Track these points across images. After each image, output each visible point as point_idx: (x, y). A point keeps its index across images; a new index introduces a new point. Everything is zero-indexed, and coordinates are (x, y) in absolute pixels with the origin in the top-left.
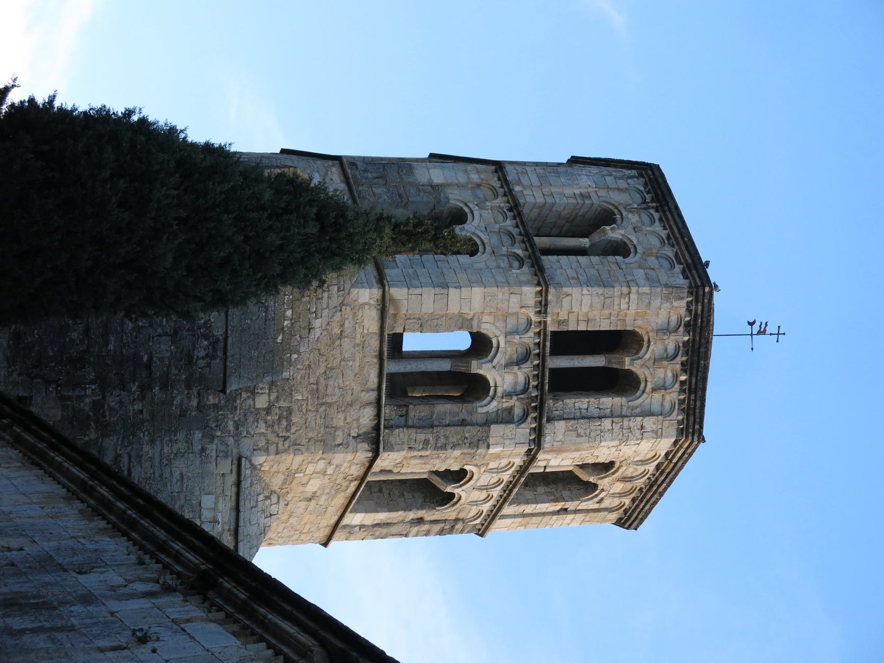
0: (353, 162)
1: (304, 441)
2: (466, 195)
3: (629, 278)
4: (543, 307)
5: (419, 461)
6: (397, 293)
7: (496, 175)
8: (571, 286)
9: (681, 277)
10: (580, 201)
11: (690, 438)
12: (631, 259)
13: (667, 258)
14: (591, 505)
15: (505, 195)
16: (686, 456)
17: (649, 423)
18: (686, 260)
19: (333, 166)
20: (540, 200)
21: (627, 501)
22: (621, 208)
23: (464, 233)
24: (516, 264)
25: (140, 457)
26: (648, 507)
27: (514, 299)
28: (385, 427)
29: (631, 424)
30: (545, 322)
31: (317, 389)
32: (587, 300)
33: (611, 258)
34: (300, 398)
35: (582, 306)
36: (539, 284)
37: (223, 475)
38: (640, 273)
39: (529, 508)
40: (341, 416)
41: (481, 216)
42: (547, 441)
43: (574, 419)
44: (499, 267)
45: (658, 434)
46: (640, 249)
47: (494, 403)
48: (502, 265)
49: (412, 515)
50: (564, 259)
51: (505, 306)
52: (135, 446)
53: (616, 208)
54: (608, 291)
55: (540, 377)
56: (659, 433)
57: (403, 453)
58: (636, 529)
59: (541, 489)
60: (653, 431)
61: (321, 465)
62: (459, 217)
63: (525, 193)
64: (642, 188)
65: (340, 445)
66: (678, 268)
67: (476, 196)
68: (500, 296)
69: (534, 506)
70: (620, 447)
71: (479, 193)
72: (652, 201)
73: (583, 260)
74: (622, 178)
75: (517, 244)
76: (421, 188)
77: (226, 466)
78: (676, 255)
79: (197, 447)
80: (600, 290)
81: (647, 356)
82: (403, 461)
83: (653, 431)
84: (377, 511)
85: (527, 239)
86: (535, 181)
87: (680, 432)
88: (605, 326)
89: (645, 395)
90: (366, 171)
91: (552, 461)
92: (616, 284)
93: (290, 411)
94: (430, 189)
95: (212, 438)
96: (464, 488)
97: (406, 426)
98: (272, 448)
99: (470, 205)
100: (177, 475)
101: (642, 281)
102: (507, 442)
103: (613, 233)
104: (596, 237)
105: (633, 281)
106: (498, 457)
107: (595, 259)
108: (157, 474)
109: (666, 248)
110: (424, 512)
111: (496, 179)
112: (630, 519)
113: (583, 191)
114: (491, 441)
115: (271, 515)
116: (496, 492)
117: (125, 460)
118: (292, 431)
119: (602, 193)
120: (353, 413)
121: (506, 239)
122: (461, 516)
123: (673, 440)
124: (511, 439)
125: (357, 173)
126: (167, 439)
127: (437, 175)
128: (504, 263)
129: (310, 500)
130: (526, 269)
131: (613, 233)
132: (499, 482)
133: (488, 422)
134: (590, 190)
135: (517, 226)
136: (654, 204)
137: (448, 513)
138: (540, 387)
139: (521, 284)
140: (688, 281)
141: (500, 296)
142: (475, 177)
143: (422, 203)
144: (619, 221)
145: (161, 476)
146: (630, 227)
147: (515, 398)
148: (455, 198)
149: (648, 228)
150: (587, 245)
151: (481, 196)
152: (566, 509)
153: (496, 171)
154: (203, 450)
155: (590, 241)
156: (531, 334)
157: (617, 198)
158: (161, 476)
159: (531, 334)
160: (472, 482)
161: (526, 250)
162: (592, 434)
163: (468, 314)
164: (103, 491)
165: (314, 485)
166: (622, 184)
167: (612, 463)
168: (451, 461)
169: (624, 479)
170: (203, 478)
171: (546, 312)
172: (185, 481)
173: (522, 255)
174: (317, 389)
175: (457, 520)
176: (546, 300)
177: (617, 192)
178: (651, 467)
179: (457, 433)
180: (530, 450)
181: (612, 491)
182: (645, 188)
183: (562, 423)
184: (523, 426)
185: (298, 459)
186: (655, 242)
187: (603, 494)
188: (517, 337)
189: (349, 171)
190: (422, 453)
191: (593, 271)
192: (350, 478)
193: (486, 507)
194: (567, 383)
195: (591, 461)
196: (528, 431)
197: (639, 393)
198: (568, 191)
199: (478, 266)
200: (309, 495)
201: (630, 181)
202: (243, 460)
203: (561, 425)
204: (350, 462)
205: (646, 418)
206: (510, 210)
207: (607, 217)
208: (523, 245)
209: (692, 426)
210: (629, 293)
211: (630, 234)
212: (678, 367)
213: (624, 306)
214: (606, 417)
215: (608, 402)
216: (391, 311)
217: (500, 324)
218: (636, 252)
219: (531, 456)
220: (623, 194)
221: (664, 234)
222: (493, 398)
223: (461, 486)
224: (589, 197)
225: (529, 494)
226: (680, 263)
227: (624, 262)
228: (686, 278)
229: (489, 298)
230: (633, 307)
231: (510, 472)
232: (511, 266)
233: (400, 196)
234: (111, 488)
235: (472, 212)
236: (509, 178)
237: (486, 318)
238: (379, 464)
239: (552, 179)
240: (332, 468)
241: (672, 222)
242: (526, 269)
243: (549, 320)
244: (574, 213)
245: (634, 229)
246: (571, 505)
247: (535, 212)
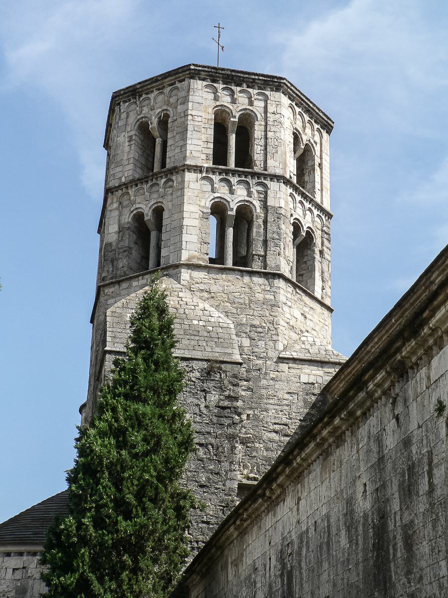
0: (101, 278)
1: (271, 318)
2: (126, 212)
3: (182, 115)
4: (197, 169)
5: (287, 249)
6: (185, 257)
7: (114, 193)
8: (186, 150)
9: (183, 82)
10: (134, 142)
11: (282, 85)
12: (171, 114)
13: (171, 91)
14: (317, 148)
15: (127, 188)
16: (292, 88)
17: (271, 109)
18: (173, 80)
19: (104, 291)
20: (131, 166)
21: (316, 126)
22: (139, 117)
23: (150, 214)
24: (170, 183)
25: (275, 418)
26: (321, 114)
27: (192, 185)
28: (266, 269)
29: (272, 120)
30: (207, 168)
31: (240, 308)
32: (195, 142)
33: (170, 125)
34: (245, 319)
35: (198, 146)
36: (184, 171)
37: (289, 368)
38: (180, 108)
39: (318, 186)
40: (257, 295)
41: (139, 203)
42: (279, 172)
43: (266, 155)
44: (172, 194)
45: (278, 104)
46: (165, 107)
47: (254, 202)
48: (171, 192)
49: (317, 256)
50: (168, 154)
51: (196, 192)
52: (269, 420)
53: (138, 121)
54: (190, 128)
55: (240, 174)
56: (278, 103)
57: (282, 259)
58: (333, 123)
59: (306, 178)
60: (277, 107)
61: (286, 309)
62: (139, 217)
63: (126, 175)
64: (127, 104)
65: (275, 297)
66: (178, 85)
67: (126, 207)
68: (189, 194)
69: (316, 183)
70: (285, 128)
71: (125, 204)
72: (135, 98)
73: (170, 142)
74: (120, 116)
75: (158, 182)
76: (120, 239)
77: (284, 367)
79: (271, 382)
80: (189, 133)
81: (231, 107)
82: (285, 259)
83: (277, 107)
84: (314, 279)
85: (156, 176)
86: (120, 169)
87: (278, 90)
88: (211, 132)
89: (254, 110)
90: (108, 271)
91: (291, 169)
92: (186, 123)
93: (253, 326)
94: (120, 233)
95: (266, 374)
96: (303, 225)
97: (265, 256)
98: (275, 338)
100: (287, 396)
101: (184, 107)
102: (278, 196)
103: (154, 124)
104: (156, 134)
105: (184, 112)
106: (287, 202)
107: (169, 135)
108: (286, 408)
109: (165, 91)
110: (316, 250)
111: (117, 193)
112: (327, 126)
113: (127, 140)
114: (277, 205)
115: (314, 341)
116: (307, 205)
117: (277, 427)
118: (265, 325)
119: (129, 129)
120: (257, 289)
121: (154, 189)
122: (320, 227)
123: (282, 95)
124: (277, 193)
125: (109, 276)
126: (265, 401)
127: (112, 228)
128: (170, 191)
129: (305, 317)
130: (174, 178)
131: (154, 124)
132: (301, 202)
133: (265, 207)
134: (126, 136)
135: (147, 182)
136: (137, 97)
137: (318, 235)
138: (246, 174)
139: (183, 181)
140: (186, 79)
141: (189, 194)
142: (115, 205)
143: (129, 240)
144: (147, 119)
145: (288, 405)
146: (151, 112)
147: (252, 190)
148: (127, 218)
149: (152, 101)
150: (161, 140)
151: (127, 202)
152: (319, 164)
153: (112, 193)
154: (273, 379)
155: (158, 137)
156: (213, 177)
157: (132, 119)
158: (288, 405)
159: (213, 177)
160: (301, 219)
161: (162, 177)
162: (276, 144)
163: (200, 215)
164: (325, 433)
165: (297, 314)
166: (124, 116)
167: (294, 133)
168: (287, 230)
169: (304, 128)
170: (290, 380)
171: (201, 167)
172: (291, 391)
173: (165, 179)
174: (240, 308)
175: (322, 231)
176: (194, 166)
177: (129, 119)
178: (298, 110)
179: (271, 226)
180: (284, 183)
181: (311, 136)
182: (127, 102)
183: (268, 161)
184: (269, 186)
185: (282, 323)
186: (161, 98)
187: (312, 141)
188: (215, 185)
189: (108, 282)
190: (282, 247)
191: (177, 137)
192: (294, 292)
193: (316, 212)
194: (244, 158)
195: (292, 146)
196: (272, 182)
197: (253, 114)
198: (127, 149)
199: (170, 207)
200: (303, 318)
201: (122, 111)
202: (281, 356)
203: (270, 162)
204: (284, 291)
205: (268, 110)
206: (137, 185)
207: (143, 128)
208: (159, 179)
209: (274, 83)
210: (192, 115)
211: (155, 113)
212: (239, 89)
213: (199, 119)
214: (266, 135)
215: (258, 132)
216: (195, 261)
217: (207, 195)
218: (167, 110)
219: (287, 182)
220: (131, 115)
221: (156, 92)
222: (251, 203)
223: (302, 226)
224: (131, 136)
225: (309, 186)
226: (174, 83)
227: (172, 117)
228: (184, 80)
229: (191, 202)
230: (200, 114)
231: (296, 196)
232: (171, 187)
233: (125, 251)
234: (323, 428)
235: (136, 209)
236: (117, 185)
237: (203, 204)
238: (287, 274)
239: (118, 158)
240: (288, 302)
241: (149, 87)
242: (174, 178)
243: (206, 165)
244: (141, 147)
245: (152, 110)
246: (317, 161)
247: (138, 170)
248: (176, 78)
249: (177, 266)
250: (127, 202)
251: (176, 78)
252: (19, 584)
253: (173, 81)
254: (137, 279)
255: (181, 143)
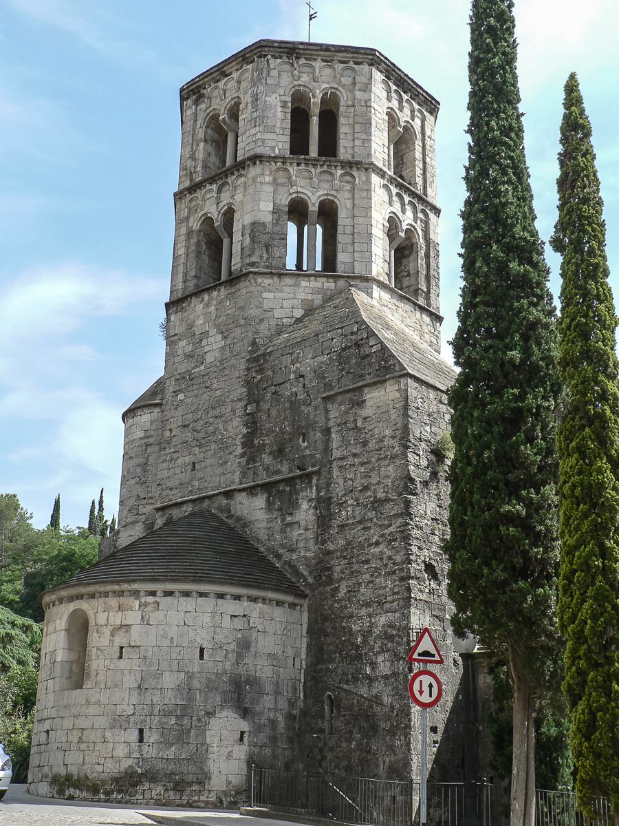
18: (349, 57)
67: (283, 185)
78: (343, 62)
99: (292, 191)
101: (366, 96)
130: (355, 174)
144: (307, 90)
151: (284, 180)
155: (316, 116)
166: (274, 73)
198: (280, 115)
218: (337, 89)
235: (297, 192)
241: (315, 53)
248: (353, 58)
249: (367, 279)
250: (284, 180)
251: (353, 58)
252: (240, 636)
253: (347, 59)
254: (307, 279)
255: (364, 136)
